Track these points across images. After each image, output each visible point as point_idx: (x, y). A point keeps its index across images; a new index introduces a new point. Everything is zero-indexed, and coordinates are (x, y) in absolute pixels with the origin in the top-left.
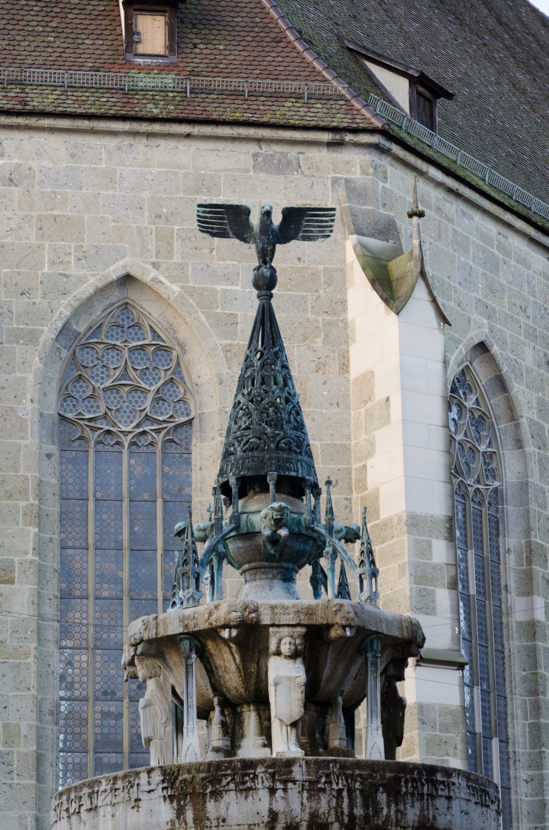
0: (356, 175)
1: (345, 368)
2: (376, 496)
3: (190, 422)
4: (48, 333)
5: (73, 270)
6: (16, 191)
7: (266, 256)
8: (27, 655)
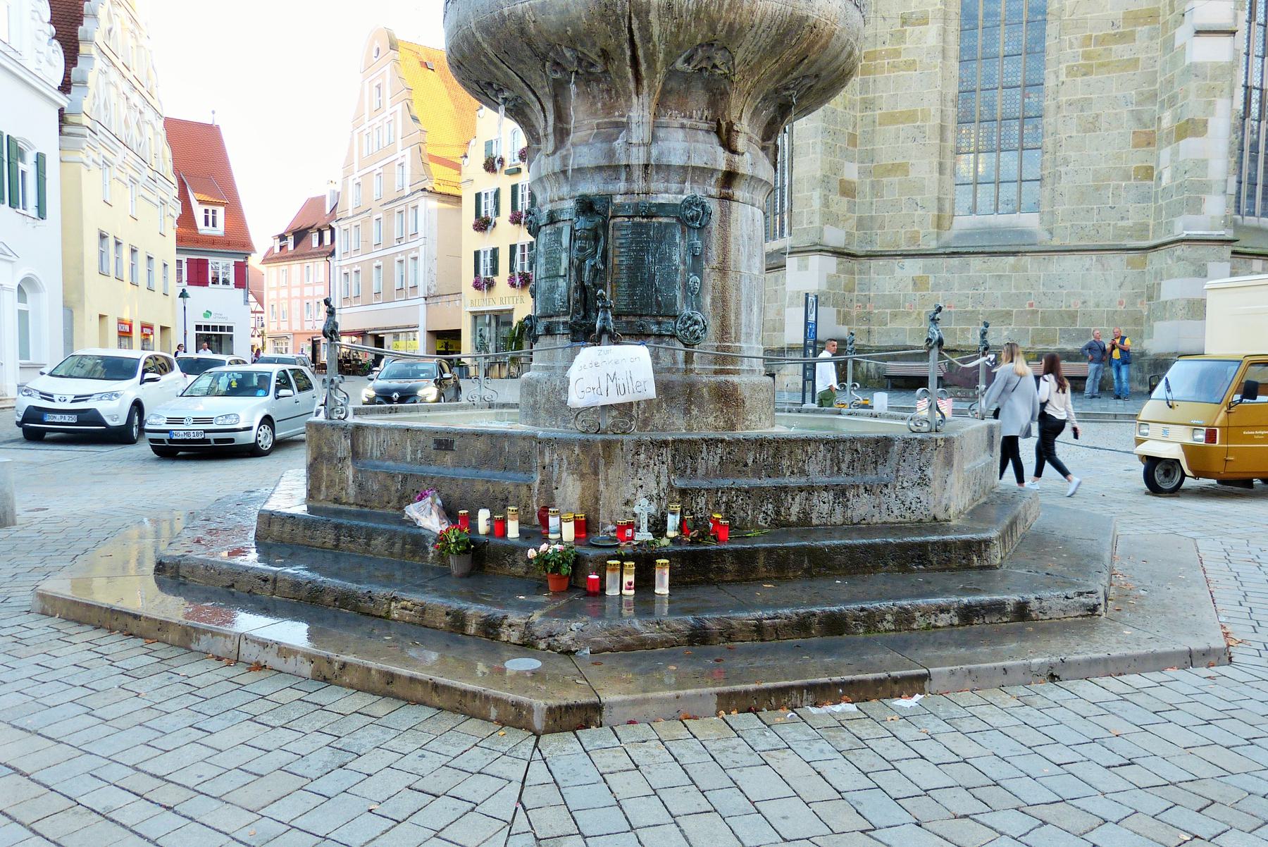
8: (935, 67)
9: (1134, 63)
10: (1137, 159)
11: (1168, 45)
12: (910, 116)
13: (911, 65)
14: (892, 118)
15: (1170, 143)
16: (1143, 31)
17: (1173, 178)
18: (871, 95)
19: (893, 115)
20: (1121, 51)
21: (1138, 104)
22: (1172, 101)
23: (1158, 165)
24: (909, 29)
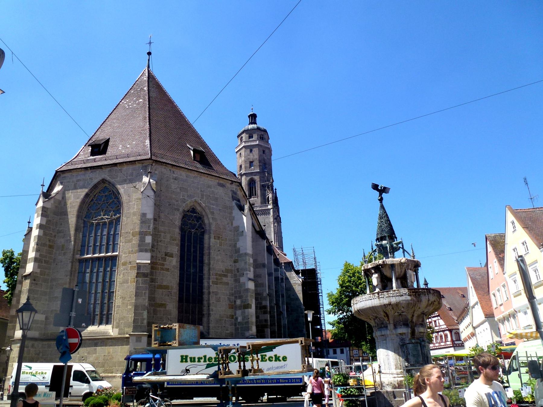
0: (234, 190)
1: (232, 224)
2: (239, 249)
3: (204, 231)
4: (181, 210)
5: (186, 198)
6: (176, 181)
7: (380, 195)
9: (227, 284)
10: (230, 312)
11: (237, 281)
12: (167, 287)
13: (168, 270)
14: (161, 287)
15: (241, 309)
16: (229, 275)
17: (243, 319)
18: (154, 277)
19: (161, 286)
20: (225, 279)
21: (230, 296)
22: (240, 297)
23: (235, 314)
24: (167, 258)
